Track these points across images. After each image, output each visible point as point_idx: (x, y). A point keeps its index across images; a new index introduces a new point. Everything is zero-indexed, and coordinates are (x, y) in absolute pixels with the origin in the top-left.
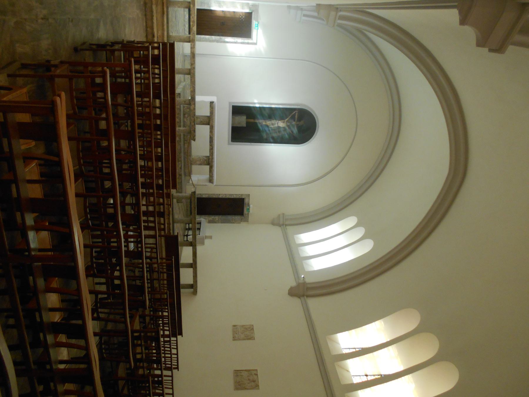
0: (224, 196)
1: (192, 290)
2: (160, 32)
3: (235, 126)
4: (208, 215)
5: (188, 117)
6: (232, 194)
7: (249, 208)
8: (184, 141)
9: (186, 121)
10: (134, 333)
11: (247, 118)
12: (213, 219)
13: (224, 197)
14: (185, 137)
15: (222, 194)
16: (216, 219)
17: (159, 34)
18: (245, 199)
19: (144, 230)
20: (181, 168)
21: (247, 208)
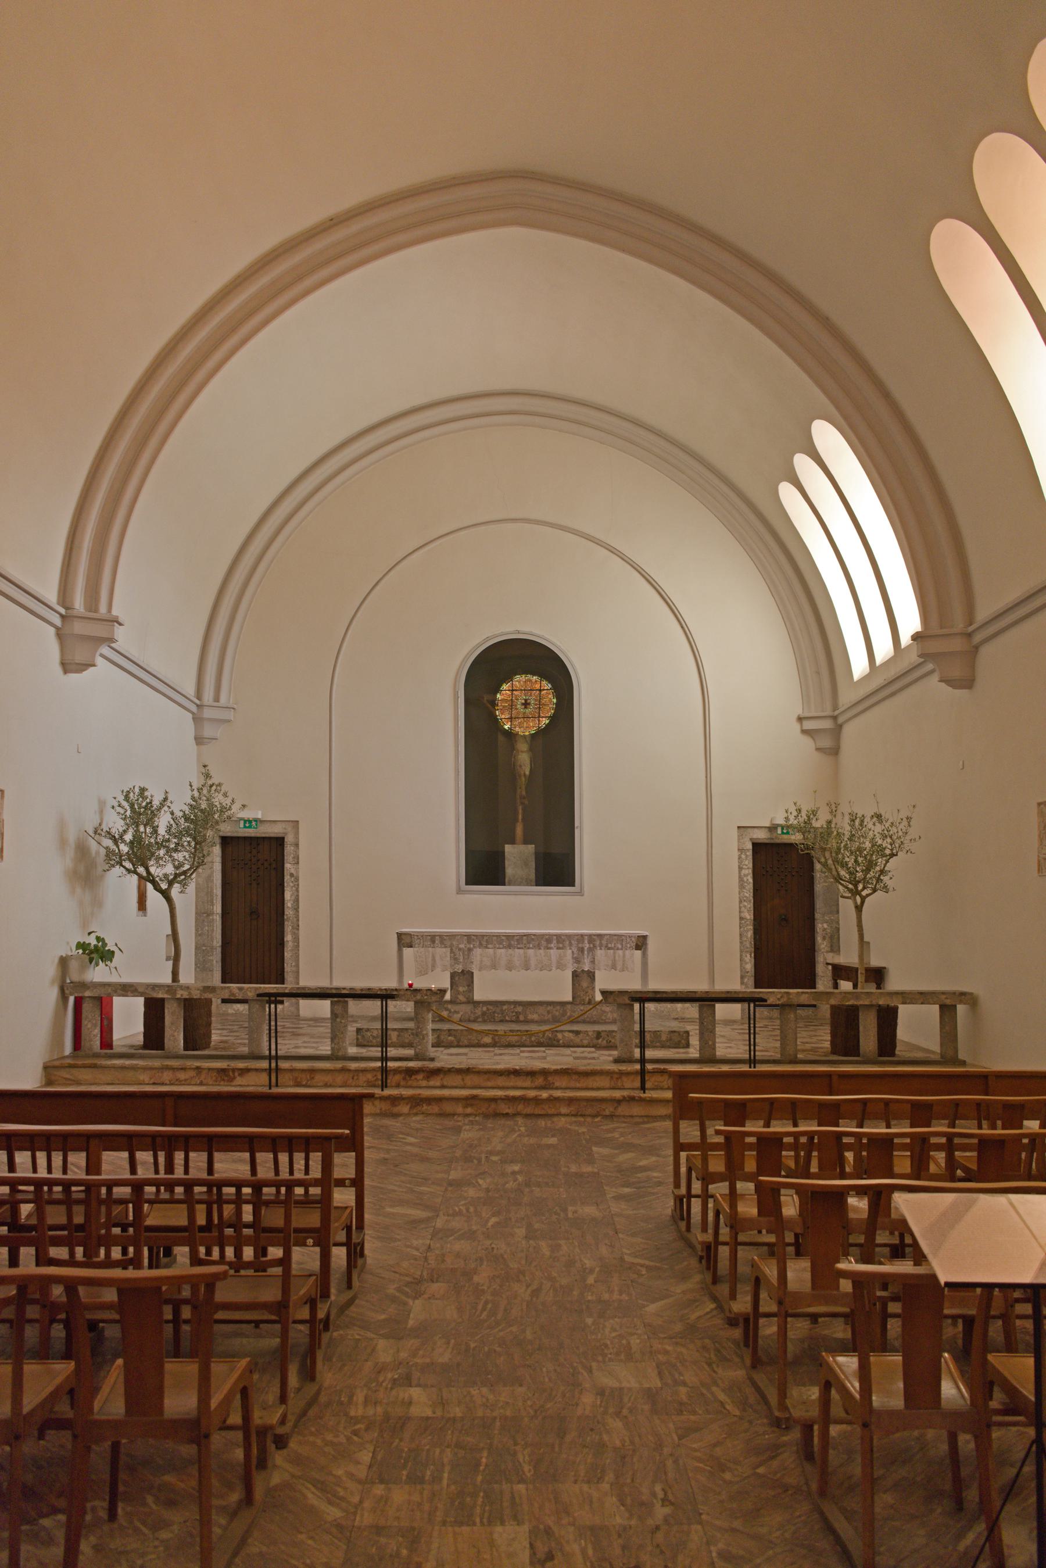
0: (745, 906)
1: (961, 1009)
2: (141, 1078)
3: (533, 876)
4: (816, 953)
5: (447, 1009)
6: (739, 881)
7: (245, 821)
8: (517, 1021)
9: (459, 1016)
10: (270, 1246)
11: (513, 842)
12: (824, 938)
13: (750, 905)
14: (507, 1018)
15: (740, 912)
16: (824, 930)
17: (147, 1080)
18: (755, 841)
19: (99, 1173)
20: (577, 1033)
21: (245, 827)
